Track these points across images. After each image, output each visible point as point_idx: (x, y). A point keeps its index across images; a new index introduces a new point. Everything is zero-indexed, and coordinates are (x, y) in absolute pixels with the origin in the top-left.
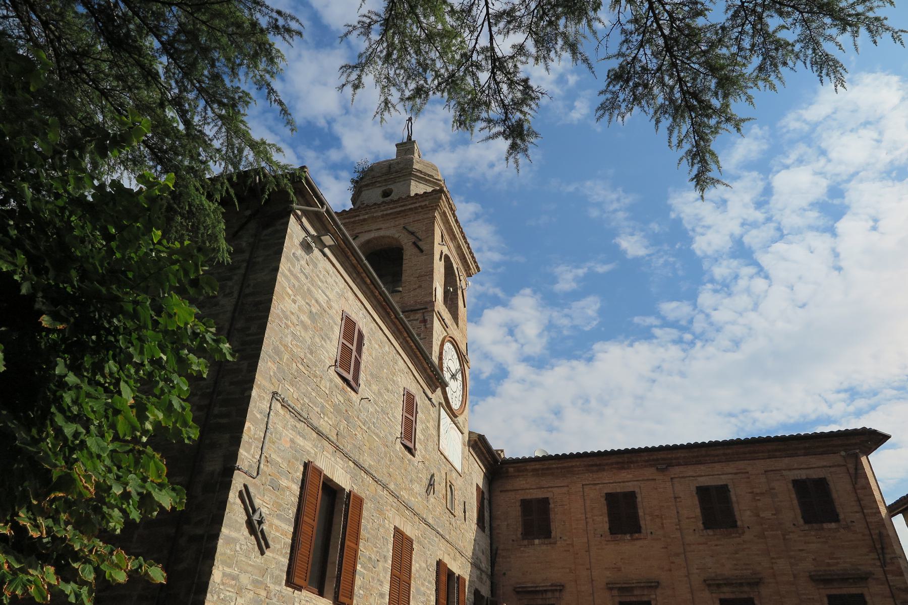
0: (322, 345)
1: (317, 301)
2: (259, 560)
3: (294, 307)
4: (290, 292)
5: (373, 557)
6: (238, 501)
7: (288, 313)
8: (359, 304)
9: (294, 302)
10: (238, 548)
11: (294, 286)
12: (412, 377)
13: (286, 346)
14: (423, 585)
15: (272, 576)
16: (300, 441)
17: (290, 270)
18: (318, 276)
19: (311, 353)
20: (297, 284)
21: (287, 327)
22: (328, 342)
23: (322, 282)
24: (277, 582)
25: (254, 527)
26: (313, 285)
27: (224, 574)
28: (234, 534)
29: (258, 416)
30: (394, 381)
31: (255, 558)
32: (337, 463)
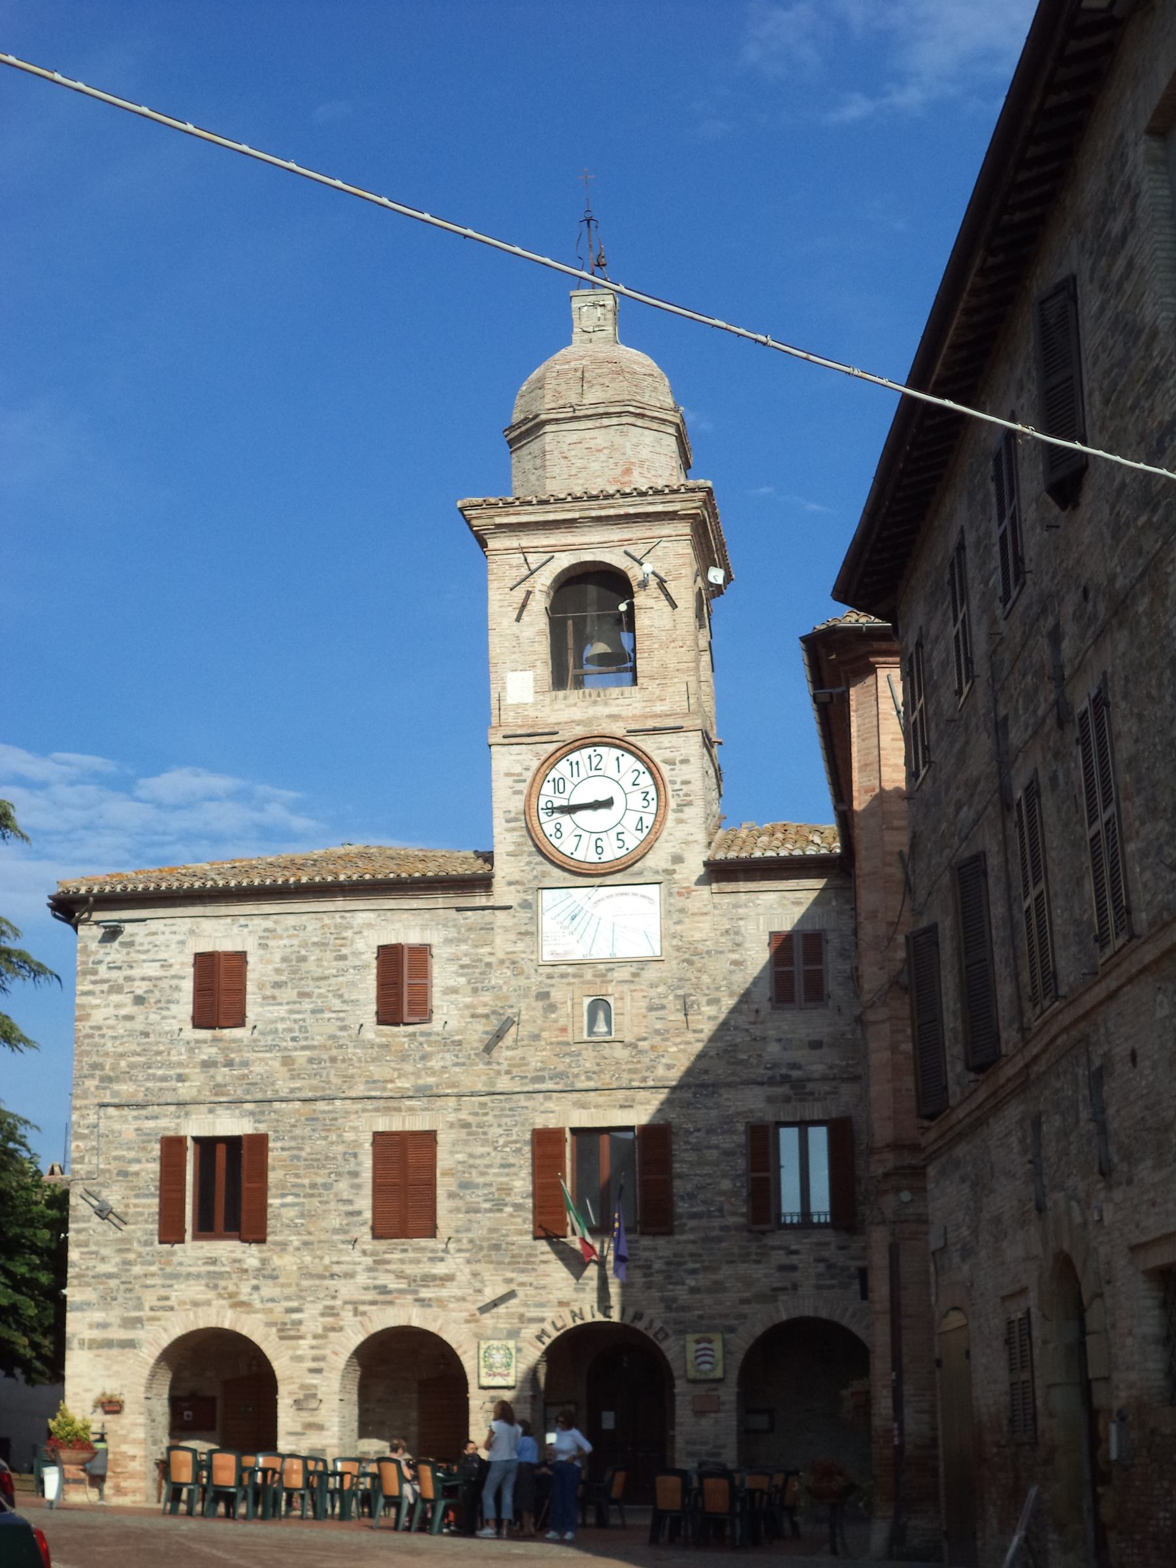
0: (164, 1018)
1: (143, 979)
2: (119, 1234)
3: (111, 1011)
4: (98, 1002)
5: (320, 1180)
6: (81, 1201)
7: (101, 1022)
8: (229, 920)
9: (107, 1006)
10: (91, 1232)
11: (102, 992)
12: (405, 915)
13: (107, 1054)
14: (483, 1174)
15: (140, 1242)
16: (151, 1124)
17: (95, 982)
18: (139, 951)
19: (147, 1035)
20: (105, 987)
21: (103, 1036)
22: (172, 1006)
23: (148, 951)
24: (147, 1243)
25: (103, 1212)
26: (131, 967)
27: (82, 1253)
28: (82, 1225)
29: (86, 1131)
30: (343, 958)
31: (113, 1234)
32: (219, 1116)
